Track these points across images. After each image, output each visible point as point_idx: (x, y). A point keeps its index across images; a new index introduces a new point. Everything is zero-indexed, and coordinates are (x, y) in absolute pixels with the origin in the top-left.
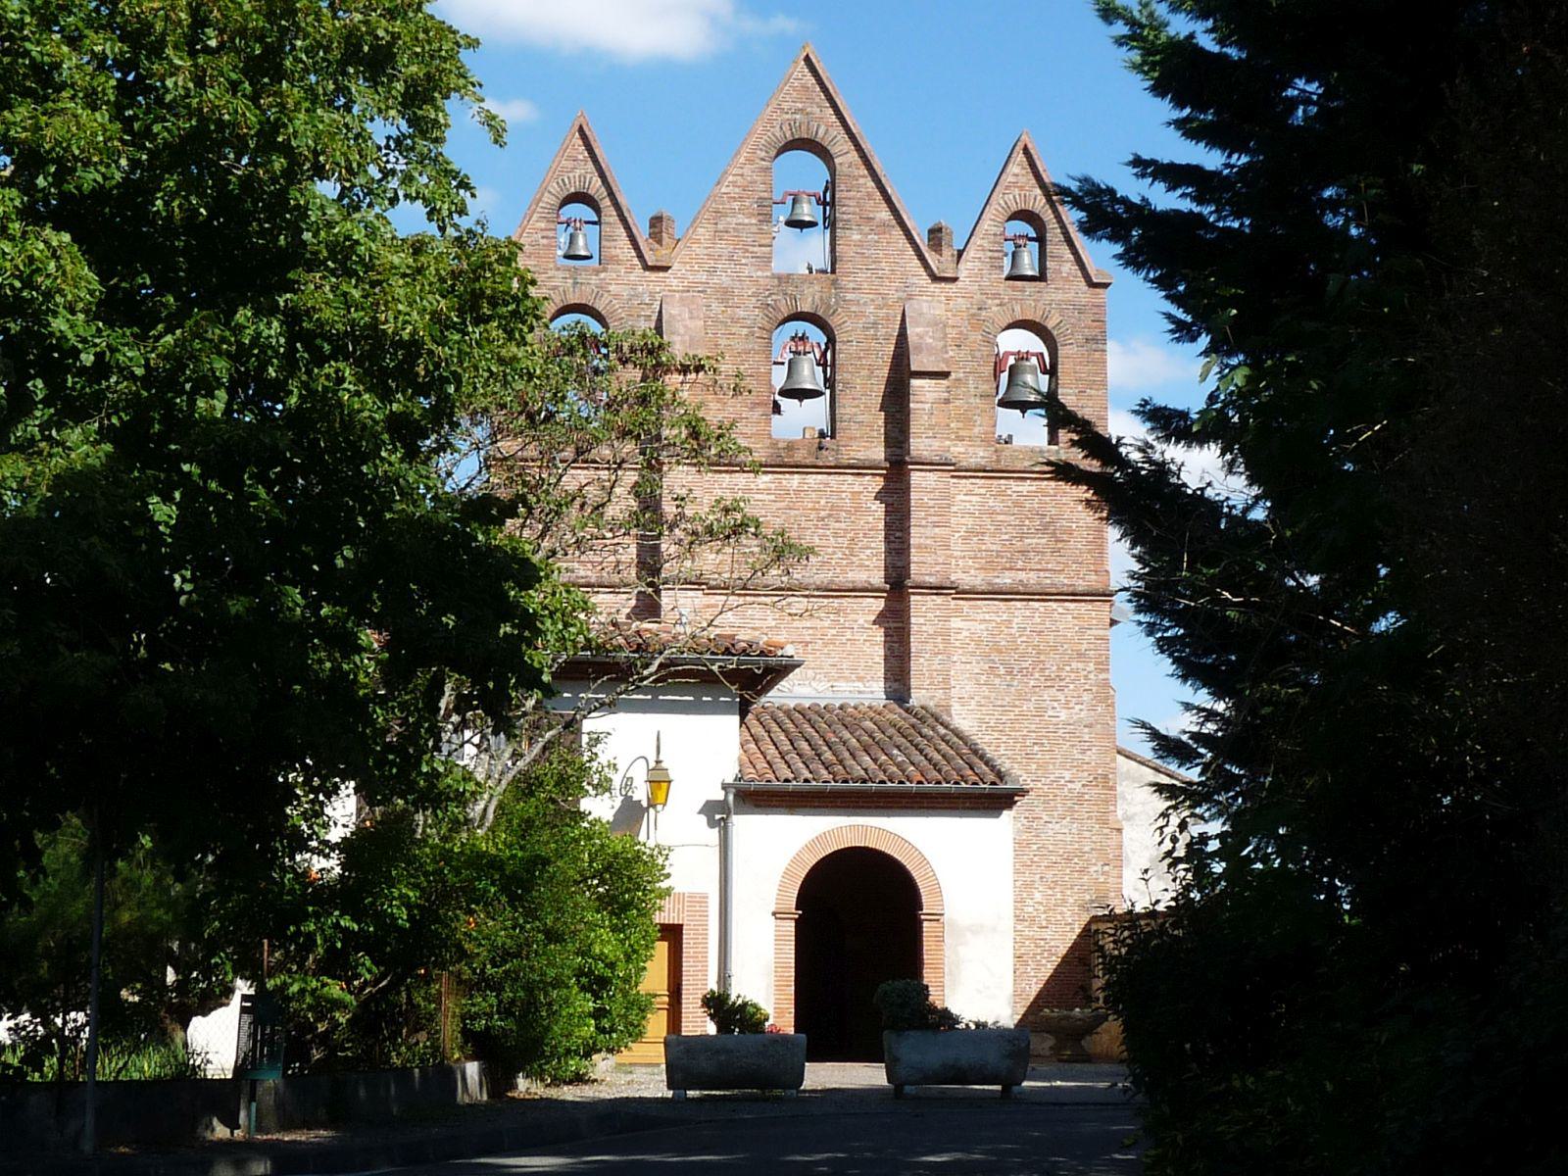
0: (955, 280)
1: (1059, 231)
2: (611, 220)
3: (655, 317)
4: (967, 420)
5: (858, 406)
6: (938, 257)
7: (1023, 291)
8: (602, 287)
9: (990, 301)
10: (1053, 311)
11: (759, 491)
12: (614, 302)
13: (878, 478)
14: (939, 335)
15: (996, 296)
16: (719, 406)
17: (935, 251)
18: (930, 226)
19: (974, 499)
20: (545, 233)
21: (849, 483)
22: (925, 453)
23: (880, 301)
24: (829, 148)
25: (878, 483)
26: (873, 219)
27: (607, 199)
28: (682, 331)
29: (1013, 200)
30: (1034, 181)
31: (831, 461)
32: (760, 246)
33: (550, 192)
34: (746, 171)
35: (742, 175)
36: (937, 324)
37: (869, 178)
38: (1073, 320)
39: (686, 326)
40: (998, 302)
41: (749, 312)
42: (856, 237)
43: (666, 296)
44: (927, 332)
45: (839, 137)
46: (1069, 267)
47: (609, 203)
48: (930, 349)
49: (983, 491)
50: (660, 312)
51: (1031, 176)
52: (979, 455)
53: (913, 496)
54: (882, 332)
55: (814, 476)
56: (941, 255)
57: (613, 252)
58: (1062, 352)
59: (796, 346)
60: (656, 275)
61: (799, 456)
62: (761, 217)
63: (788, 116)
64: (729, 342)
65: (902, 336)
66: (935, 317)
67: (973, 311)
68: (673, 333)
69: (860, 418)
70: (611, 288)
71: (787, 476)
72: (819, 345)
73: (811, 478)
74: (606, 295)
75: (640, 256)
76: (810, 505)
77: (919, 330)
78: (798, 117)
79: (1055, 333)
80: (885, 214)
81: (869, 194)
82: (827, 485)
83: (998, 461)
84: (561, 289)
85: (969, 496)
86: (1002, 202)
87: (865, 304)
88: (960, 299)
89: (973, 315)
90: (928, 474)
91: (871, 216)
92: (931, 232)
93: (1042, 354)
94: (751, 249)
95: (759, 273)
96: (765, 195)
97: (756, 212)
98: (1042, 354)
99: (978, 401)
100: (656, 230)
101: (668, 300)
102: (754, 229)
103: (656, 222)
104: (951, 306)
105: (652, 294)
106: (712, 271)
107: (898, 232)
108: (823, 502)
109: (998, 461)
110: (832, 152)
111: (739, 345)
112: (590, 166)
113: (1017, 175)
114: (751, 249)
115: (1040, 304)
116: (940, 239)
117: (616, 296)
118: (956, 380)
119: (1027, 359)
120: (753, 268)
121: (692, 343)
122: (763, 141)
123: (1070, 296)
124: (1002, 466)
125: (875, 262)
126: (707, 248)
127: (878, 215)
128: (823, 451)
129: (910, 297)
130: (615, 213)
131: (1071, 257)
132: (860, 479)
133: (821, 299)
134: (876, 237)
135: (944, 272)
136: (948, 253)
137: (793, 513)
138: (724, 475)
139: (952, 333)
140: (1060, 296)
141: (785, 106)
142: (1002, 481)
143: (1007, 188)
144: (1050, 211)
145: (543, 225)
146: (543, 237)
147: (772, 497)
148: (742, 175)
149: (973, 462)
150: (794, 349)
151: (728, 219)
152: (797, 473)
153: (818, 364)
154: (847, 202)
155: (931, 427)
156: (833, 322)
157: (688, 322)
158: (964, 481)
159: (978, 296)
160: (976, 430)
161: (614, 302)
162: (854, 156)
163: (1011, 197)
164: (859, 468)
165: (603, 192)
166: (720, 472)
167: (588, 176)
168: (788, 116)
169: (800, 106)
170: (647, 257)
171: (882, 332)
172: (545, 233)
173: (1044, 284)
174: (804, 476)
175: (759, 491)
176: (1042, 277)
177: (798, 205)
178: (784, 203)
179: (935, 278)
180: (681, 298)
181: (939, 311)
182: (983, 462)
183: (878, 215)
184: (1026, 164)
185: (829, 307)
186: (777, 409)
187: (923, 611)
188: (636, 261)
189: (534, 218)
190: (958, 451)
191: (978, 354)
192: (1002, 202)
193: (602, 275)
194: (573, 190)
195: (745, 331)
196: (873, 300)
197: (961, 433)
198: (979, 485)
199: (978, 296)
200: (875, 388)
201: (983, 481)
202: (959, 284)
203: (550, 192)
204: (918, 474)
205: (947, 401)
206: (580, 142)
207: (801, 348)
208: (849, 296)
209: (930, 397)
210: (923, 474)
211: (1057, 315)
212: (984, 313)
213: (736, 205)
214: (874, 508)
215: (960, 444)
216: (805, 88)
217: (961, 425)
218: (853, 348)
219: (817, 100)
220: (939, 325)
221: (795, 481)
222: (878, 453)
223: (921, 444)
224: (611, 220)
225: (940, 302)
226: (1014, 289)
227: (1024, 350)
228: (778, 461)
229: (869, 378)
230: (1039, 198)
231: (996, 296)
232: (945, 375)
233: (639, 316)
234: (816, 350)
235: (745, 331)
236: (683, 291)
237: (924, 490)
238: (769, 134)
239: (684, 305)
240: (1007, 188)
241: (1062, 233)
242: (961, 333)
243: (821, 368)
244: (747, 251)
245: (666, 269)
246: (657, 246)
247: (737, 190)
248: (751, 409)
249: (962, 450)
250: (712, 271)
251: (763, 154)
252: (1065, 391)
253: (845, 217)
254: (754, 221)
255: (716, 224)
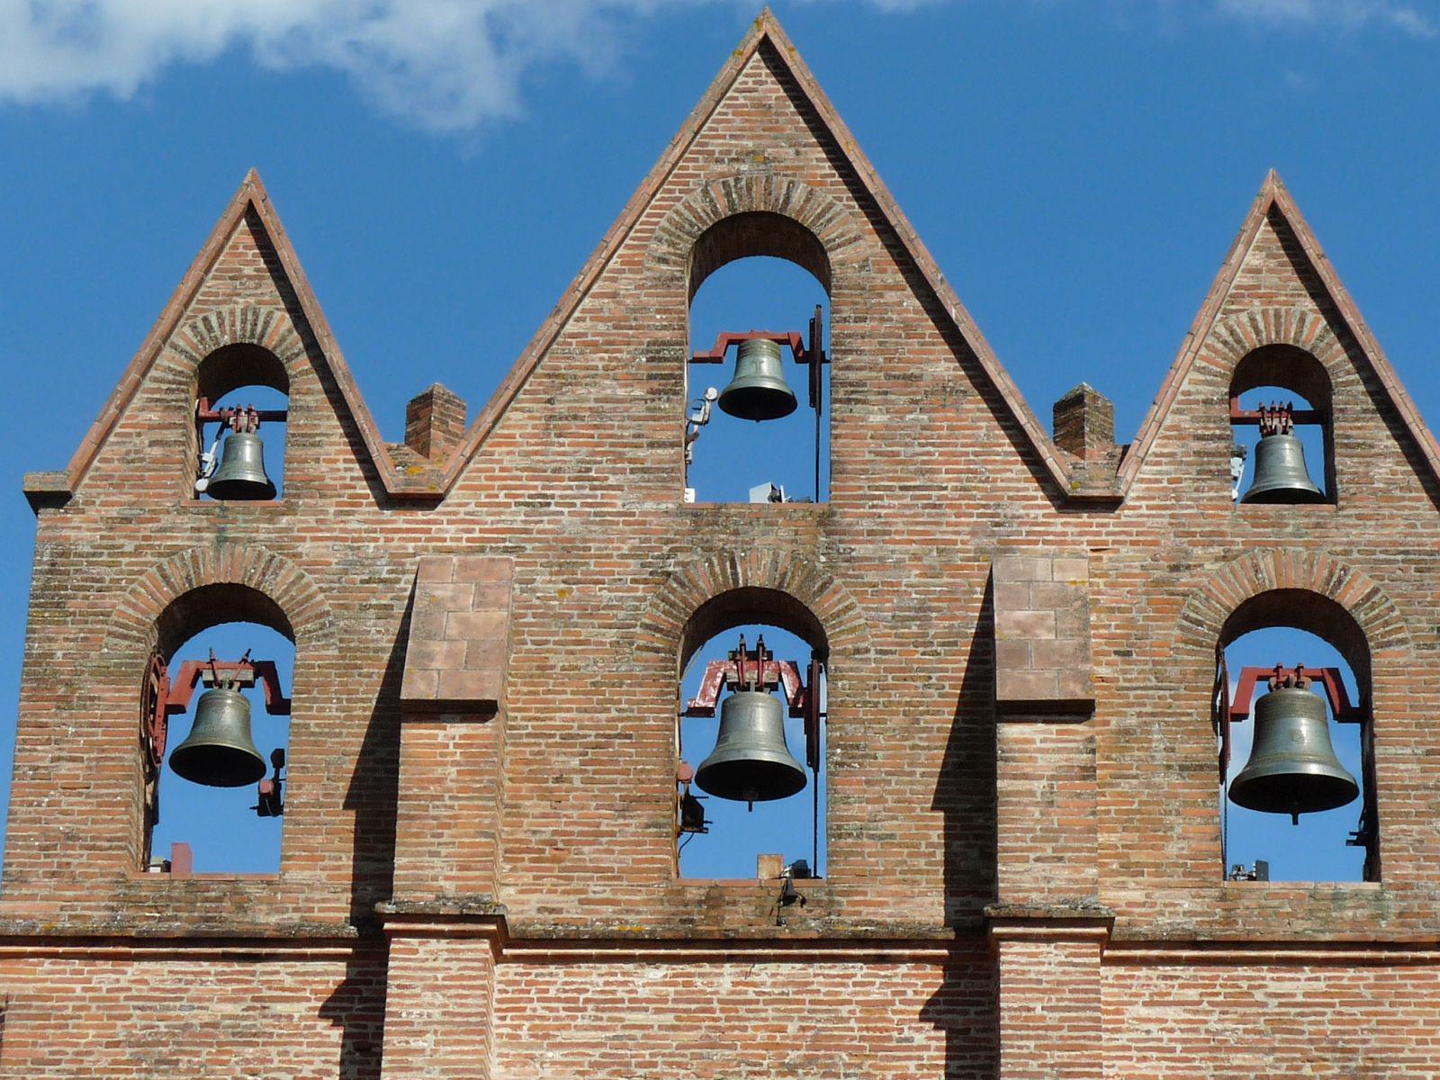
0: (1112, 504)
1: (1362, 388)
2: (310, 400)
3: (399, 611)
4: (1151, 827)
5: (881, 800)
6: (1075, 459)
7: (1280, 524)
8: (283, 548)
9: (1199, 551)
10: (1354, 569)
11: (637, 1004)
12: (309, 577)
13: (929, 969)
14: (1070, 623)
15: (1213, 537)
16: (545, 806)
17: (1069, 449)
18: (1059, 396)
19: (1171, 1013)
20: (157, 435)
21: (857, 982)
22: (1034, 895)
23: (933, 558)
24: (815, 230)
25: (925, 982)
26: (919, 377)
27: (304, 357)
28: (453, 630)
29: (1252, 325)
30: (1297, 283)
31: (814, 928)
32: (651, 445)
33: (175, 347)
34: (625, 285)
35: (614, 295)
36: (1065, 601)
37: (909, 291)
38: (1405, 588)
39: (464, 622)
40: (1218, 550)
41: (627, 596)
42: (877, 418)
43: (429, 562)
44: (1043, 618)
45: (839, 206)
46: (1389, 467)
47: (308, 366)
48: (1048, 656)
49: (1193, 994)
50: (412, 598)
51: (1289, 271)
52: (1182, 908)
53: (1007, 1001)
54: (938, 626)
55: (772, 967)
56: (1081, 455)
57: (311, 469)
58: (1380, 660)
59: (740, 671)
60: (409, 516)
61: (738, 919)
62: (655, 384)
63: (719, 168)
64: (572, 660)
65: (986, 630)
66: (1067, 589)
67: (1157, 574)
68: (430, 637)
69: (887, 826)
70: (305, 548)
71: (707, 968)
72: (794, 666)
73: (764, 973)
74: (290, 563)
75: (373, 476)
76: (761, 1036)
77: (1020, 615)
78: (744, 167)
79: (1361, 617)
80: (945, 367)
81: (908, 327)
82: (803, 986)
83: (1228, 921)
84: (188, 554)
85: (1153, 1011)
86: (1222, 330)
87: (899, 564)
88: (1123, 549)
89: (1158, 583)
90: (1044, 948)
91: (914, 371)
92: (1060, 407)
93: (1334, 673)
94: (630, 453)
95: (649, 506)
96: (667, 335)
97: (644, 373)
98: (1334, 673)
99: (1174, 779)
100: (420, 424)
101: (432, 569)
102: (639, 409)
103: (420, 408)
104: (1105, 564)
105: (397, 560)
106: (538, 505)
107: (975, 406)
108: (792, 1028)
109: (1228, 921)
110: (822, 237)
111: (595, 667)
112: (269, 287)
113: (1258, 271)
114: (630, 453)
115: (1322, 555)
116: (1081, 421)
117: (313, 565)
118: (1119, 732)
119: (1299, 685)
120: (633, 496)
121: (473, 658)
122: (664, 222)
123: (1396, 531)
124: (1238, 931)
125: (923, 473)
126: (527, 454)
127: (930, 369)
128: (797, 909)
129: (1006, 548)
130: (319, 386)
131: (1393, 444)
132: (885, 971)
133: (794, 557)
134: (925, 417)
135: (1083, 486)
136: (1096, 451)
137: (718, 1054)
138: (552, 968)
139: (1105, 625)
140: (1370, 533)
141: (716, 146)
142: (1241, 971)
143: (1234, 298)
144: (1338, 346)
145: (154, 417)
146: (153, 444)
147: (669, 1019)
148: (614, 295)
149: (1164, 924)
150: (733, 677)
151: (581, 391)
152: (731, 959)
153: (794, 713)
154: (857, 344)
155: (1049, 835)
156: (822, 607)
157: (471, 614)
158: (1144, 971)
159: (1169, 541)
160: (1172, 849)
161: (309, 577)
162: (873, 245)
163: (1244, 318)
164: (880, 945)
165: (296, 341)
166: (543, 960)
167: (264, 310)
168: (719, 168)
169: (750, 144)
170: (385, 475)
171: (938, 626)
172: (157, 435)
173: (1331, 507)
174: (746, 968)
175: (637, 1004)
176: (1329, 496)
177: (746, 361)
178: (718, 360)
179: (1067, 503)
180: (464, 566)
181: (1074, 573)
182: (1191, 924)
183: (930, 369)
184: (1276, 246)
185: (811, 575)
186: (693, 817)
187: (421, 973)
188: (363, 488)
189: (137, 401)
190: (1123, 898)
191: (1173, 671)
192: (1222, 330)
193: (284, 521)
194: (226, 340)
195: (611, 635)
196: (916, 557)
197: (1135, 856)
198: (1185, 981)
199: (1169, 541)
200: (923, 756)
201: (1191, 971)
202: (1124, 514)
203: (175, 347)
204: (1018, 947)
205: (1088, 772)
206: (250, 240)
207: (751, 676)
208: (861, 550)
209: (1046, 763)
210: (1031, 947)
211: (1366, 576)
212: (1185, 578)
213: (598, 360)
214: (919, 1039)
215: (1131, 882)
216: (762, 107)
217: (1134, 837)
218: (868, 667)
219: (789, 130)
220: (1078, 605)
221: (726, 977)
222: (928, 907)
223: (1024, 877)
224: (310, 400)
225: (1079, 556)
226: (1256, 521)
227: (1289, 664)
228: (683, 931)
229: (907, 732)
230: (1310, 318)
231: (1213, 537)
232: (1079, 710)
233: (364, 608)
234: (787, 680)
235: (611, 635)
236: (471, 551)
237: (1036, 986)
238: (679, 206)
239: (465, 580)
240: (1234, 298)
241: (1371, 394)
242: (1130, 623)
243: (801, 722)
244: (620, 457)
245: (430, 501)
246: (416, 457)
247: (601, 327)
248: (623, 812)
249: (1137, 896)
250: (538, 505)
251: (664, 249)
252: (1391, 750)
253: (852, 376)
254: (638, 393)
255: (550, 401)
